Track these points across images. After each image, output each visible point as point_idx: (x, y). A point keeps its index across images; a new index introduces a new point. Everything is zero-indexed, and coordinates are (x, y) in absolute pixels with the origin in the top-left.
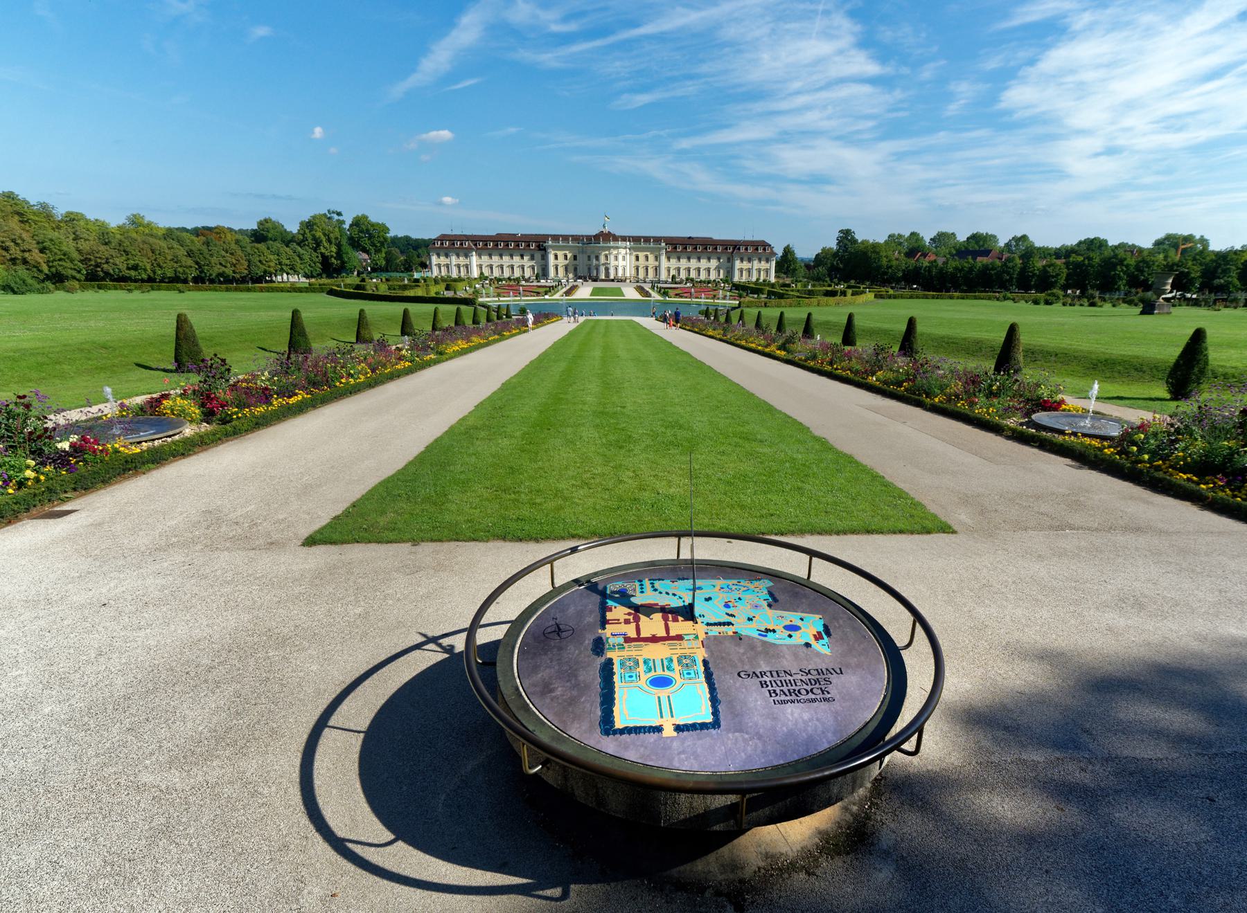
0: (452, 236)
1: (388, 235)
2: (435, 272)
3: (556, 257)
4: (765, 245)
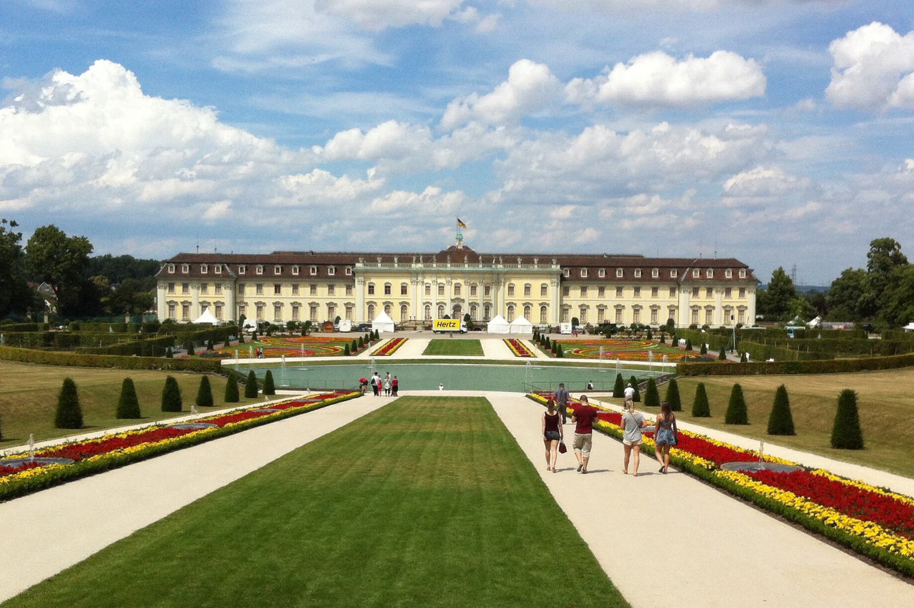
1: (89, 255)
3: (371, 290)
4: (735, 265)
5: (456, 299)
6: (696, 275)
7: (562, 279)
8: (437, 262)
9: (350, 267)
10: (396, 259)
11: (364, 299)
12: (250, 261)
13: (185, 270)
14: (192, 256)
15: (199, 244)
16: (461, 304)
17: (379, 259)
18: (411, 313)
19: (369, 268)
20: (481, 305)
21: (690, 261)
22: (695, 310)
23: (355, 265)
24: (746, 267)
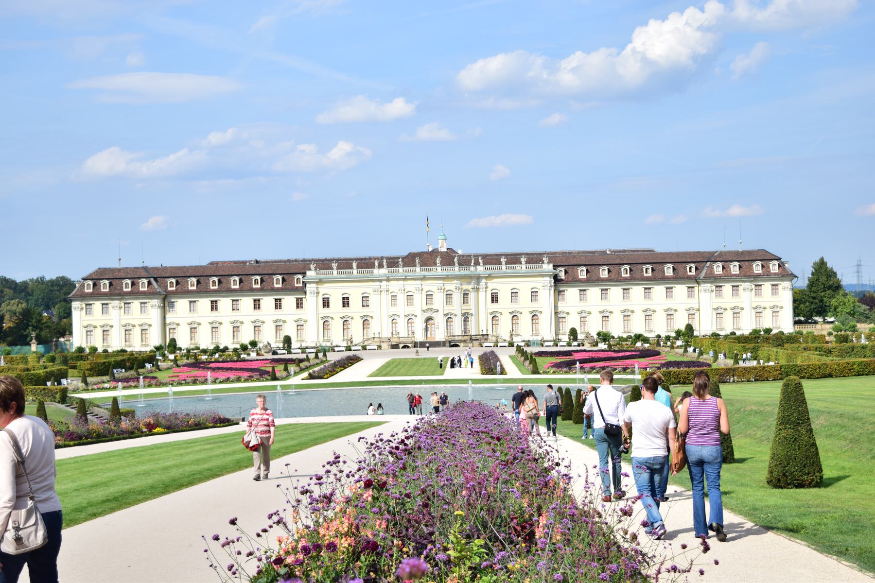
0: (119, 270)
2: (77, 340)
3: (326, 303)
4: (766, 257)
5: (428, 310)
6: (718, 269)
7: (557, 279)
8: (404, 266)
9: (300, 276)
10: (354, 265)
11: (318, 314)
12: (181, 275)
13: (104, 286)
14: (112, 270)
15: (121, 258)
16: (434, 315)
17: (334, 265)
18: (375, 328)
19: (322, 276)
20: (459, 315)
21: (712, 254)
22: (719, 313)
23: (306, 273)
24: (779, 259)
